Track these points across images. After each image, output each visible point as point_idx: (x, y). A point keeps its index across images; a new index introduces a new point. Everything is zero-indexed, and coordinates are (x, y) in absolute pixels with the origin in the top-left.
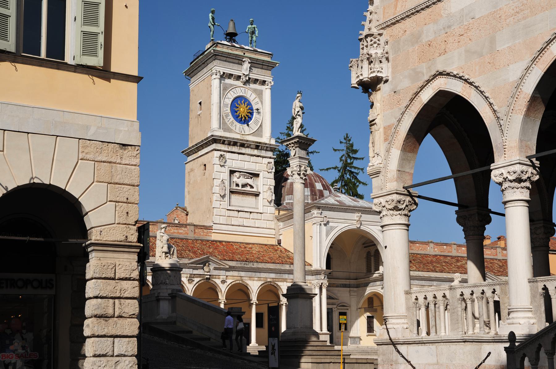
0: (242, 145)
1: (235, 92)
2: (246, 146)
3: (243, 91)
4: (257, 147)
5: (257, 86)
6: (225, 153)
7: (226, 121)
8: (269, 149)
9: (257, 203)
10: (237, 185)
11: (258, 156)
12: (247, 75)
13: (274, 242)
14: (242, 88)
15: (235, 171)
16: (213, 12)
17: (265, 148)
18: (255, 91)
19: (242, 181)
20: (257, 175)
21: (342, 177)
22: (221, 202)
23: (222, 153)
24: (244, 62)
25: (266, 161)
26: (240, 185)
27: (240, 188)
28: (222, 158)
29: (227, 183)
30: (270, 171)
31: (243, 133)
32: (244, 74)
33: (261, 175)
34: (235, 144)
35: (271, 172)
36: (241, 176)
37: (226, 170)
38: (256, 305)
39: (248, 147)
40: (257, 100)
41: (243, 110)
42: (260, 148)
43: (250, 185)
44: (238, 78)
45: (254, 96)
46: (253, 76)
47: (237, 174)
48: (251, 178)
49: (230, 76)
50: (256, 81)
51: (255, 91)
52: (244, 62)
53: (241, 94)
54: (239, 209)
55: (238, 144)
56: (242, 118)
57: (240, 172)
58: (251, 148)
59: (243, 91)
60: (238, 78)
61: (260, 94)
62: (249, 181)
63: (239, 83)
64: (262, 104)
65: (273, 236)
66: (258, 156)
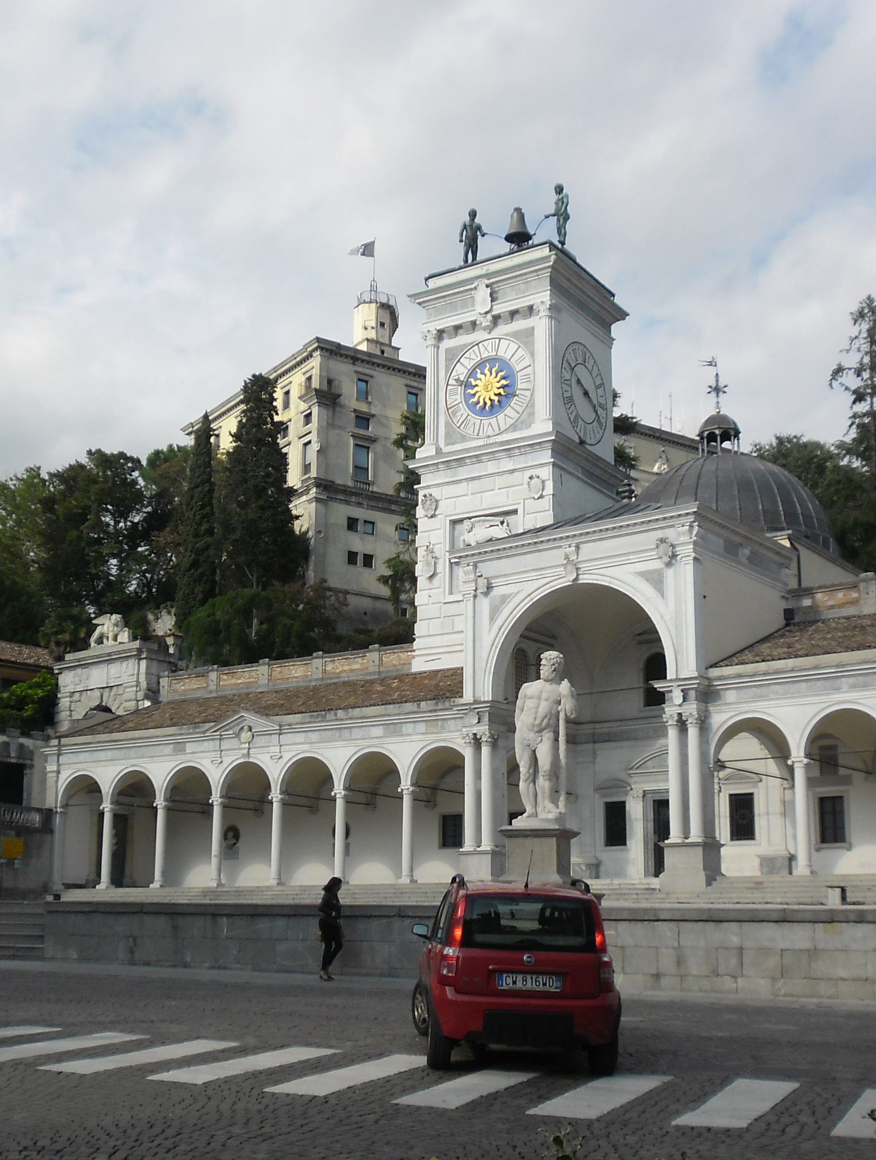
0: (478, 458)
3: (489, 349)
5: (520, 324)
11: (512, 471)
12: (487, 313)
15: (461, 521)
20: (515, 512)
22: (431, 592)
24: (475, 288)
31: (490, 432)
32: (480, 314)
41: (487, 386)
46: (500, 308)
47: (467, 523)
48: (502, 523)
49: (457, 328)
56: (485, 403)
57: (470, 518)
59: (489, 349)
63: (479, 335)
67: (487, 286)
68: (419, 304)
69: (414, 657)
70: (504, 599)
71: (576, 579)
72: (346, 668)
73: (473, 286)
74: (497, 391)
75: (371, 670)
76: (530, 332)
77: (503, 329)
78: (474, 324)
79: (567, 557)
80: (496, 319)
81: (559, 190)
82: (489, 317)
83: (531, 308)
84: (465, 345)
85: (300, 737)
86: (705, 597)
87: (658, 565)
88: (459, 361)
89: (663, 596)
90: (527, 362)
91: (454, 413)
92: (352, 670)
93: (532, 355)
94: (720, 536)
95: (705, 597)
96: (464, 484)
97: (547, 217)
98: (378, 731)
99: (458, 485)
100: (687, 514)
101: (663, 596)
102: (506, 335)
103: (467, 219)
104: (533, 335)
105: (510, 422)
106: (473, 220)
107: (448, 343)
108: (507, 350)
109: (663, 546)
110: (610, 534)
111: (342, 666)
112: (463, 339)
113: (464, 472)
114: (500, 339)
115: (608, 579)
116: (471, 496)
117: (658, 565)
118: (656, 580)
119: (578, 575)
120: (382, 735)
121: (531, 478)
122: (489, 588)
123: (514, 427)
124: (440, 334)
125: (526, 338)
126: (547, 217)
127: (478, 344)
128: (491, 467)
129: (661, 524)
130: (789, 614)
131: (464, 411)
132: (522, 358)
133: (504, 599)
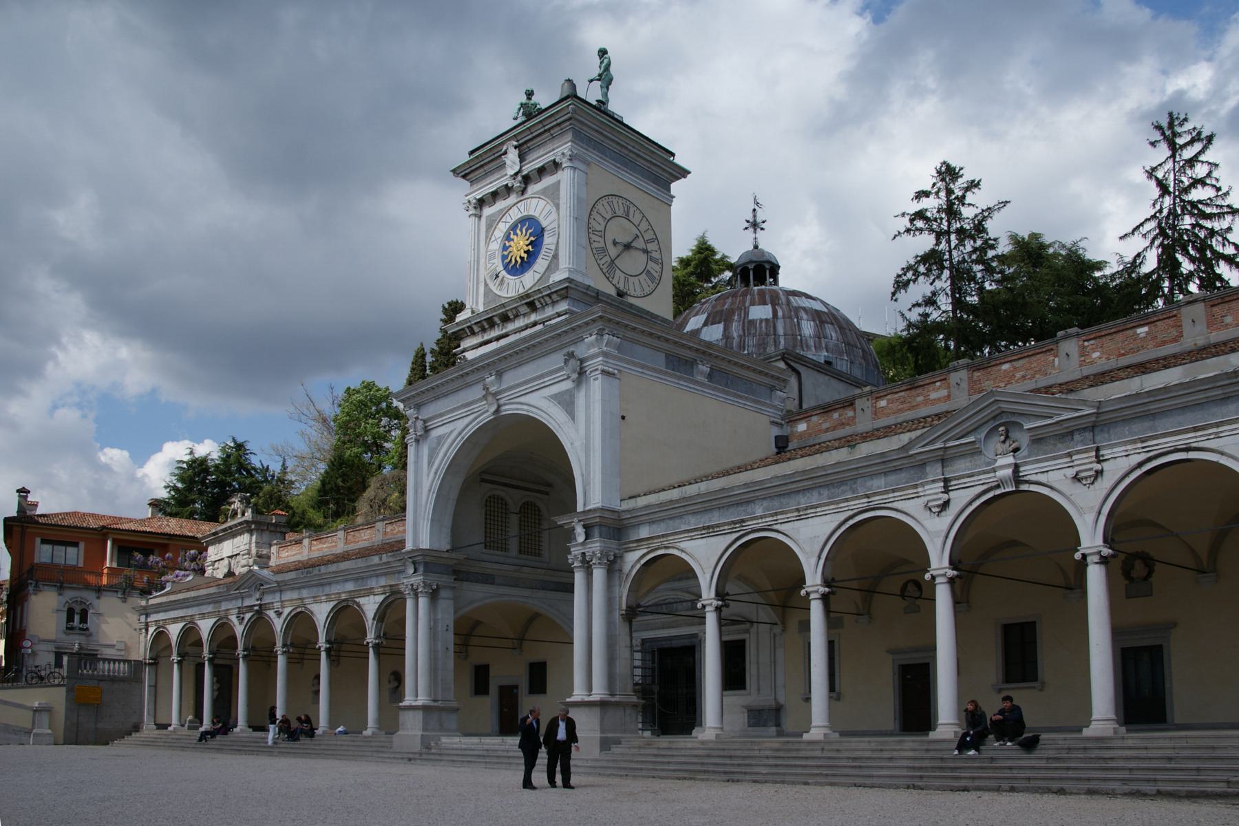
1: (509, 219)
2: (510, 314)
4: (532, 307)
5: (548, 181)
8: (555, 297)
12: (516, 174)
17: (547, 299)
39: (517, 316)
41: (520, 244)
42: (537, 303)
44: (508, 189)
46: (531, 166)
49: (495, 195)
50: (542, 171)
55: (496, 320)
58: (524, 315)
60: (508, 189)
63: (513, 199)
68: (464, 177)
71: (497, 411)
74: (526, 248)
77: (533, 189)
79: (486, 388)
80: (527, 180)
81: (603, 53)
82: (519, 178)
84: (501, 210)
86: (623, 418)
87: (567, 385)
89: (573, 419)
93: (557, 206)
94: (656, 349)
95: (623, 418)
97: (591, 81)
100: (594, 320)
101: (573, 419)
103: (524, 100)
105: (538, 276)
106: (529, 99)
107: (488, 211)
109: (572, 362)
110: (526, 355)
112: (501, 205)
115: (525, 407)
118: (567, 402)
119: (499, 406)
122: (427, 430)
124: (481, 203)
125: (552, 194)
126: (591, 81)
129: (572, 336)
130: (782, 445)
132: (550, 213)
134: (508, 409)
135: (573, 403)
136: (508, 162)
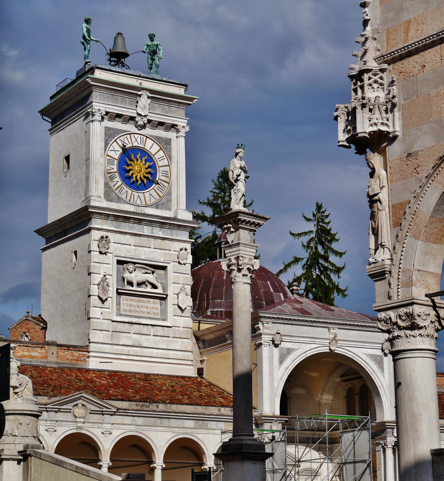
3: (139, 140)
5: (160, 133)
6: (109, 234)
7: (112, 184)
9: (164, 312)
10: (130, 283)
11: (164, 239)
12: (145, 116)
13: (192, 372)
14: (136, 136)
16: (88, 21)
18: (157, 140)
19: (137, 276)
21: (307, 276)
23: (104, 234)
24: (140, 96)
25: (177, 246)
26: (135, 283)
27: (134, 288)
28: (104, 242)
29: (113, 282)
30: (185, 262)
31: (139, 202)
33: (170, 268)
34: (126, 219)
35: (184, 264)
36: (137, 270)
37: (111, 259)
38: (163, 469)
40: (161, 153)
41: (139, 169)
43: (151, 284)
45: (156, 148)
47: (131, 267)
48: (153, 273)
51: (157, 140)
52: (140, 96)
53: (135, 144)
54: (134, 320)
57: (135, 263)
59: (139, 140)
61: (165, 145)
62: (151, 278)
63: (130, 127)
64: (170, 158)
65: (190, 363)
66: (164, 239)
67: (149, 97)
69: (89, 357)
70: (289, 351)
72: (26, 354)
73: (139, 93)
75: (50, 359)
76: (168, 142)
77: (148, 131)
78: (132, 119)
83: (173, 126)
85: (128, 420)
88: (115, 141)
90: (165, 162)
91: (111, 178)
92: (33, 357)
96: (128, 236)
98: (190, 424)
99: (124, 236)
101: (383, 371)
102: (151, 136)
104: (170, 144)
105: (153, 200)
108: (152, 148)
111: (23, 351)
113: (125, 227)
114: (147, 137)
115: (352, 354)
116: (133, 247)
117: (379, 353)
120: (193, 427)
121: (181, 250)
123: (156, 206)
127: (130, 134)
128: (146, 230)
131: (118, 179)
133: (289, 351)
134: (339, 351)
135: (382, 363)
136: (140, 103)
